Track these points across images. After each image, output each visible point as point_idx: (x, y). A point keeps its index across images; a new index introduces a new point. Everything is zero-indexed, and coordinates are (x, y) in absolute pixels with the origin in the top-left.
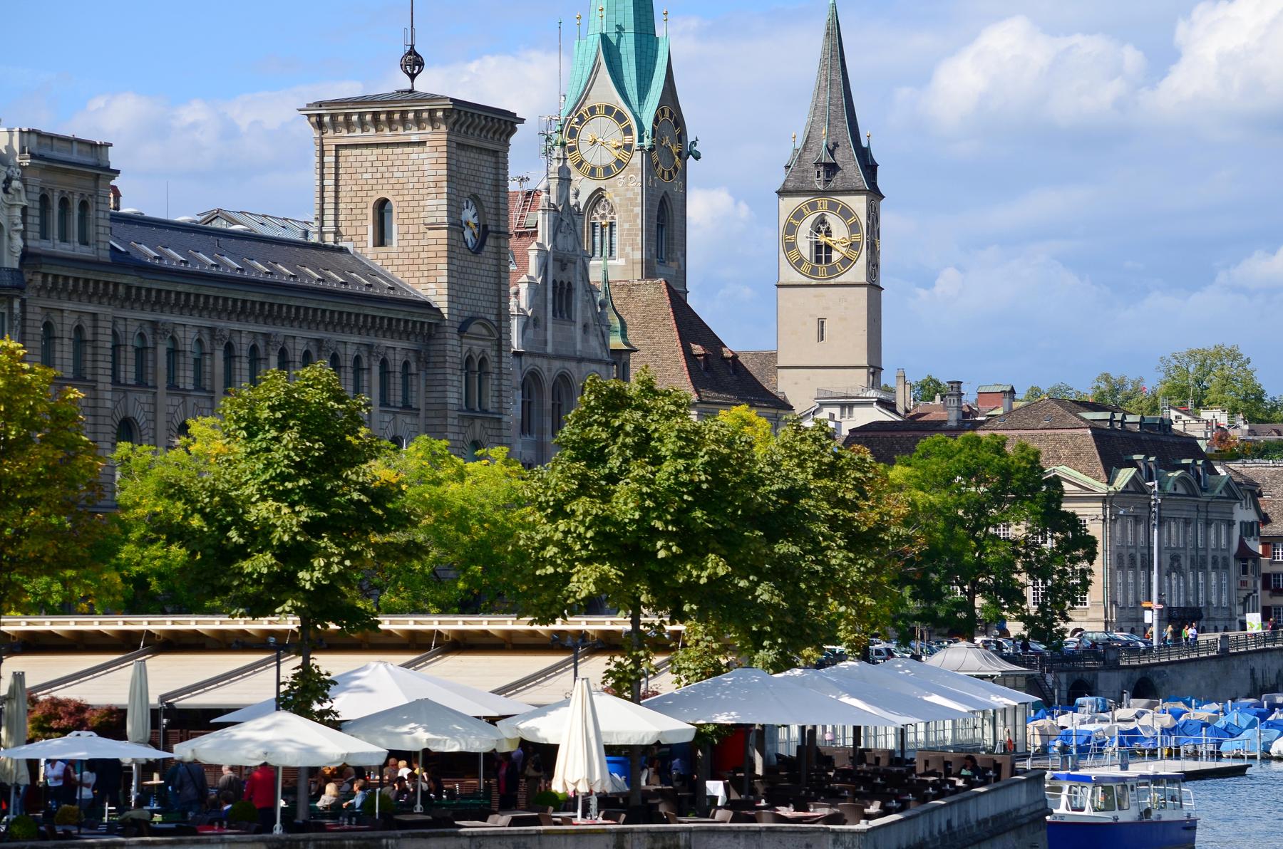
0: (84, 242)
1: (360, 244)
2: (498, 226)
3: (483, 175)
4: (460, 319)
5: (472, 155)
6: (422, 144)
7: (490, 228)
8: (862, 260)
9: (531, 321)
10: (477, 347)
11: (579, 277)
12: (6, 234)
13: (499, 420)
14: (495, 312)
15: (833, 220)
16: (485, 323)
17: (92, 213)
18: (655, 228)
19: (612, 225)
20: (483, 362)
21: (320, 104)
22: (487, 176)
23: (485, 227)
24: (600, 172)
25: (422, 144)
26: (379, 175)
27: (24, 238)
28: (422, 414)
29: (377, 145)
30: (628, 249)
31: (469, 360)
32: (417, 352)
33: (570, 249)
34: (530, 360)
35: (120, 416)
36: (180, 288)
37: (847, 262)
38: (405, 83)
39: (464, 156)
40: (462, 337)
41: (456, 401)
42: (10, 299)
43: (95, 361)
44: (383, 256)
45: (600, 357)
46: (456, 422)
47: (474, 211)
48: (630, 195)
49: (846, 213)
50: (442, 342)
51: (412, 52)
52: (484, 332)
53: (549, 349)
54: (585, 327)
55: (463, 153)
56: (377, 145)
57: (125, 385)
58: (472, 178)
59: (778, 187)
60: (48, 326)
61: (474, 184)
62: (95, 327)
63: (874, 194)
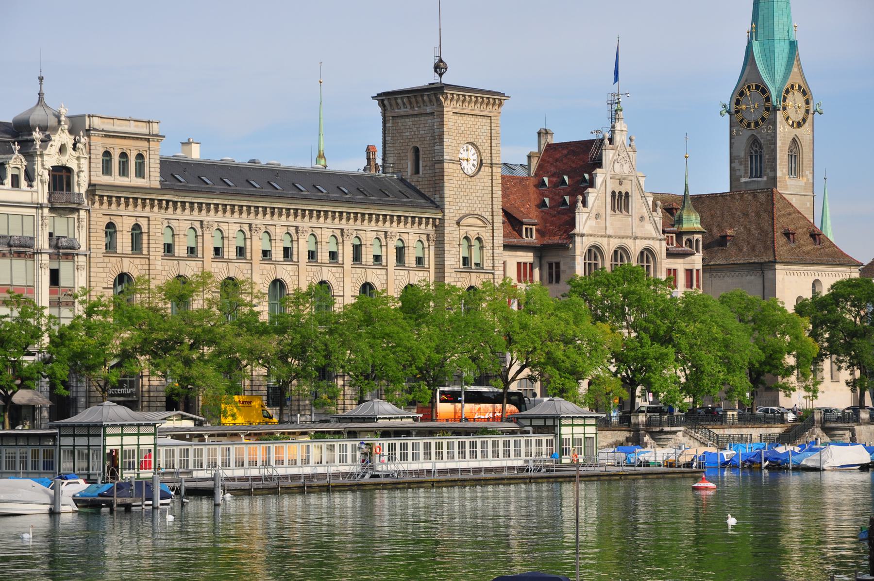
1: (404, 174)
2: (491, 160)
3: (478, 130)
4: (458, 215)
5: (469, 119)
6: (432, 114)
7: (484, 162)
9: (593, 216)
10: (473, 233)
12: (75, 173)
13: (493, 274)
14: (490, 210)
16: (479, 217)
17: (146, 160)
19: (761, 156)
22: (482, 131)
23: (481, 161)
24: (752, 125)
26: (413, 133)
27: (90, 176)
29: (412, 116)
30: (768, 171)
32: (428, 235)
33: (627, 172)
34: (592, 239)
36: (216, 201)
40: (459, 226)
41: (455, 263)
42: (78, 210)
43: (149, 243)
44: (415, 180)
45: (654, 235)
46: (454, 275)
47: (473, 151)
48: (769, 138)
50: (442, 228)
51: (441, 61)
52: (479, 223)
54: (642, 219)
55: (461, 118)
56: (412, 116)
57: (179, 257)
58: (468, 132)
60: (110, 226)
61: (470, 136)
62: (149, 224)
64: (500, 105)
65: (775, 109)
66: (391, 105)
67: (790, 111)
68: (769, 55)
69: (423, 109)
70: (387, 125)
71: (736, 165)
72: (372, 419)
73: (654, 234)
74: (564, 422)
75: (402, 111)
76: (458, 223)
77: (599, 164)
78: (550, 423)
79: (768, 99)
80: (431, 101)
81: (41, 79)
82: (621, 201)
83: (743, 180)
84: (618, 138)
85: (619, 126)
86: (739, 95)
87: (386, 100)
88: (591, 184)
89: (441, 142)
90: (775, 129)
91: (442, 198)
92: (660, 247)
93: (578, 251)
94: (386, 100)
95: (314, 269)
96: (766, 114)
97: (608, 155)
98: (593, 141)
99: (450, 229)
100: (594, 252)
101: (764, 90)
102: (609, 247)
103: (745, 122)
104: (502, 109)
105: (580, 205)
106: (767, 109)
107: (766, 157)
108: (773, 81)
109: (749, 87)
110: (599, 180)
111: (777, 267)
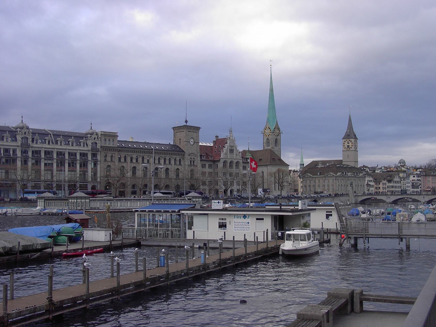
6: (183, 131)
8: (353, 147)
11: (235, 148)
15: (349, 142)
18: (274, 142)
20: (194, 159)
24: (268, 136)
25: (183, 131)
28: (183, 165)
34: (225, 159)
39: (190, 133)
42: (98, 152)
45: (240, 158)
49: (351, 141)
51: (186, 120)
52: (194, 155)
53: (229, 158)
63: (356, 138)
78: (191, 198)
81: (91, 124)
92: (241, 161)
94: (174, 128)
98: (226, 138)
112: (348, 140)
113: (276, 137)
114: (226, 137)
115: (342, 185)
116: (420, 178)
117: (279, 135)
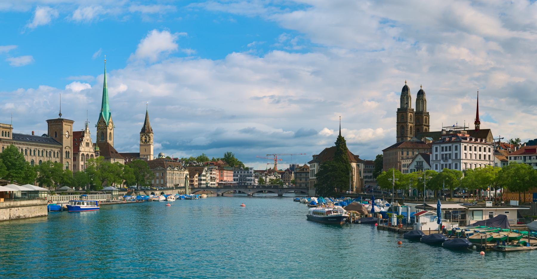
0: (9, 136)
6: (60, 125)
10: (68, 150)
15: (147, 136)
16: (69, 147)
20: (69, 152)
21: (49, 120)
31: (66, 152)
32: (59, 151)
35: (39, 160)
37: (148, 142)
38: (59, 117)
49: (148, 136)
52: (69, 148)
53: (86, 151)
59: (140, 132)
64: (73, 123)
65: (107, 126)
66: (50, 123)
67: (110, 127)
68: (105, 115)
69: (58, 124)
70: (49, 127)
71: (98, 137)
72: (66, 190)
73: (93, 152)
74: (113, 191)
75: (53, 124)
76: (65, 148)
77: (84, 137)
78: (110, 191)
79: (105, 124)
80: (60, 122)
82: (87, 144)
83: (100, 141)
84: (88, 131)
85: (87, 128)
86: (99, 122)
87: (49, 121)
88: (82, 140)
89: (62, 131)
90: (107, 130)
91: (62, 143)
92: (94, 154)
93: (80, 155)
94: (49, 121)
95: (39, 157)
96: (105, 127)
97: (85, 135)
98: (81, 132)
99: (64, 149)
100: (83, 154)
101: (105, 122)
102: (85, 154)
103: (100, 129)
104: (73, 124)
105: (80, 145)
106: (105, 126)
107: (105, 136)
108: (106, 120)
109: (101, 122)
110: (84, 140)
111: (111, 159)
112: (145, 135)
113: (110, 131)
114: (82, 131)
115: (169, 178)
116: (215, 172)
117: (113, 129)
